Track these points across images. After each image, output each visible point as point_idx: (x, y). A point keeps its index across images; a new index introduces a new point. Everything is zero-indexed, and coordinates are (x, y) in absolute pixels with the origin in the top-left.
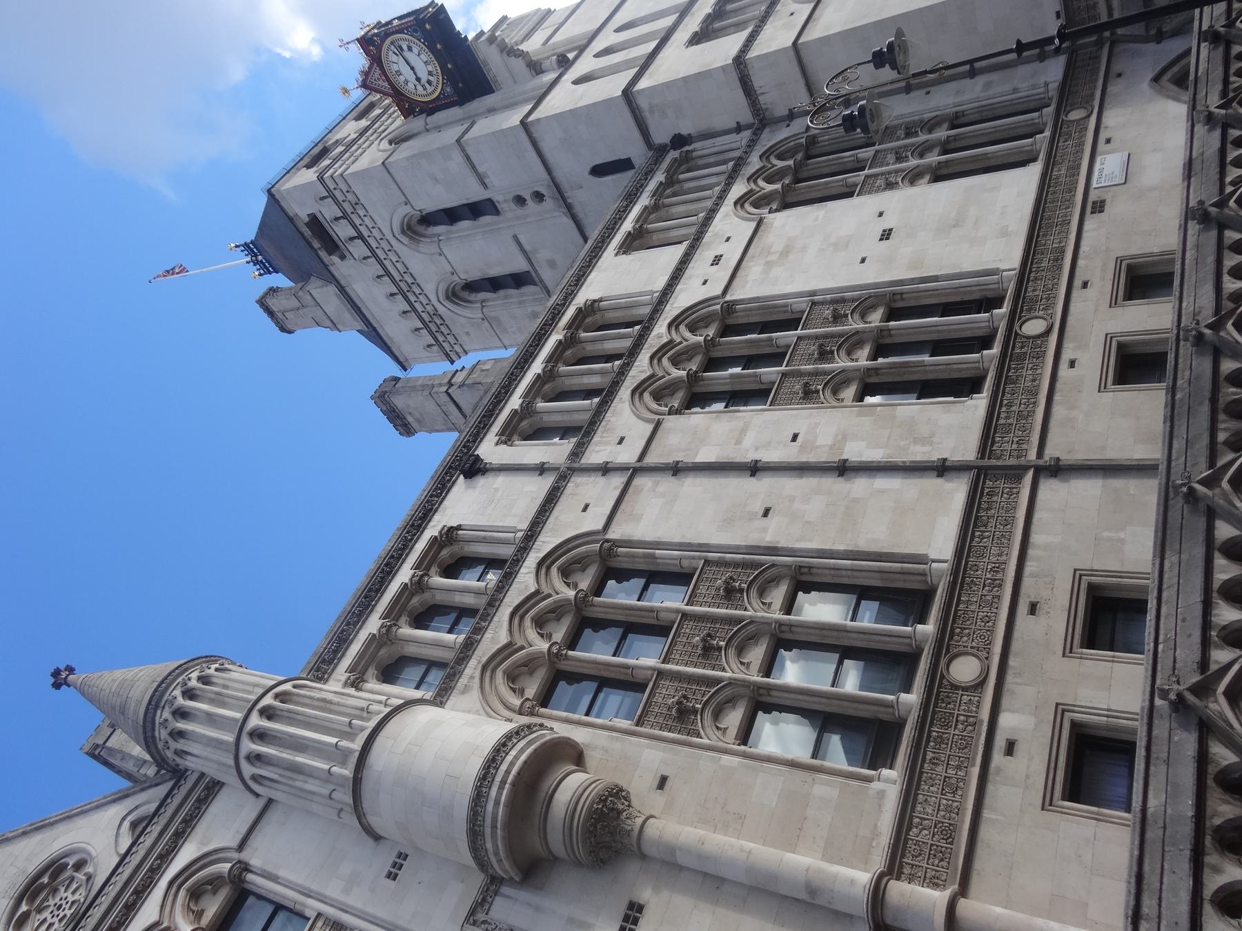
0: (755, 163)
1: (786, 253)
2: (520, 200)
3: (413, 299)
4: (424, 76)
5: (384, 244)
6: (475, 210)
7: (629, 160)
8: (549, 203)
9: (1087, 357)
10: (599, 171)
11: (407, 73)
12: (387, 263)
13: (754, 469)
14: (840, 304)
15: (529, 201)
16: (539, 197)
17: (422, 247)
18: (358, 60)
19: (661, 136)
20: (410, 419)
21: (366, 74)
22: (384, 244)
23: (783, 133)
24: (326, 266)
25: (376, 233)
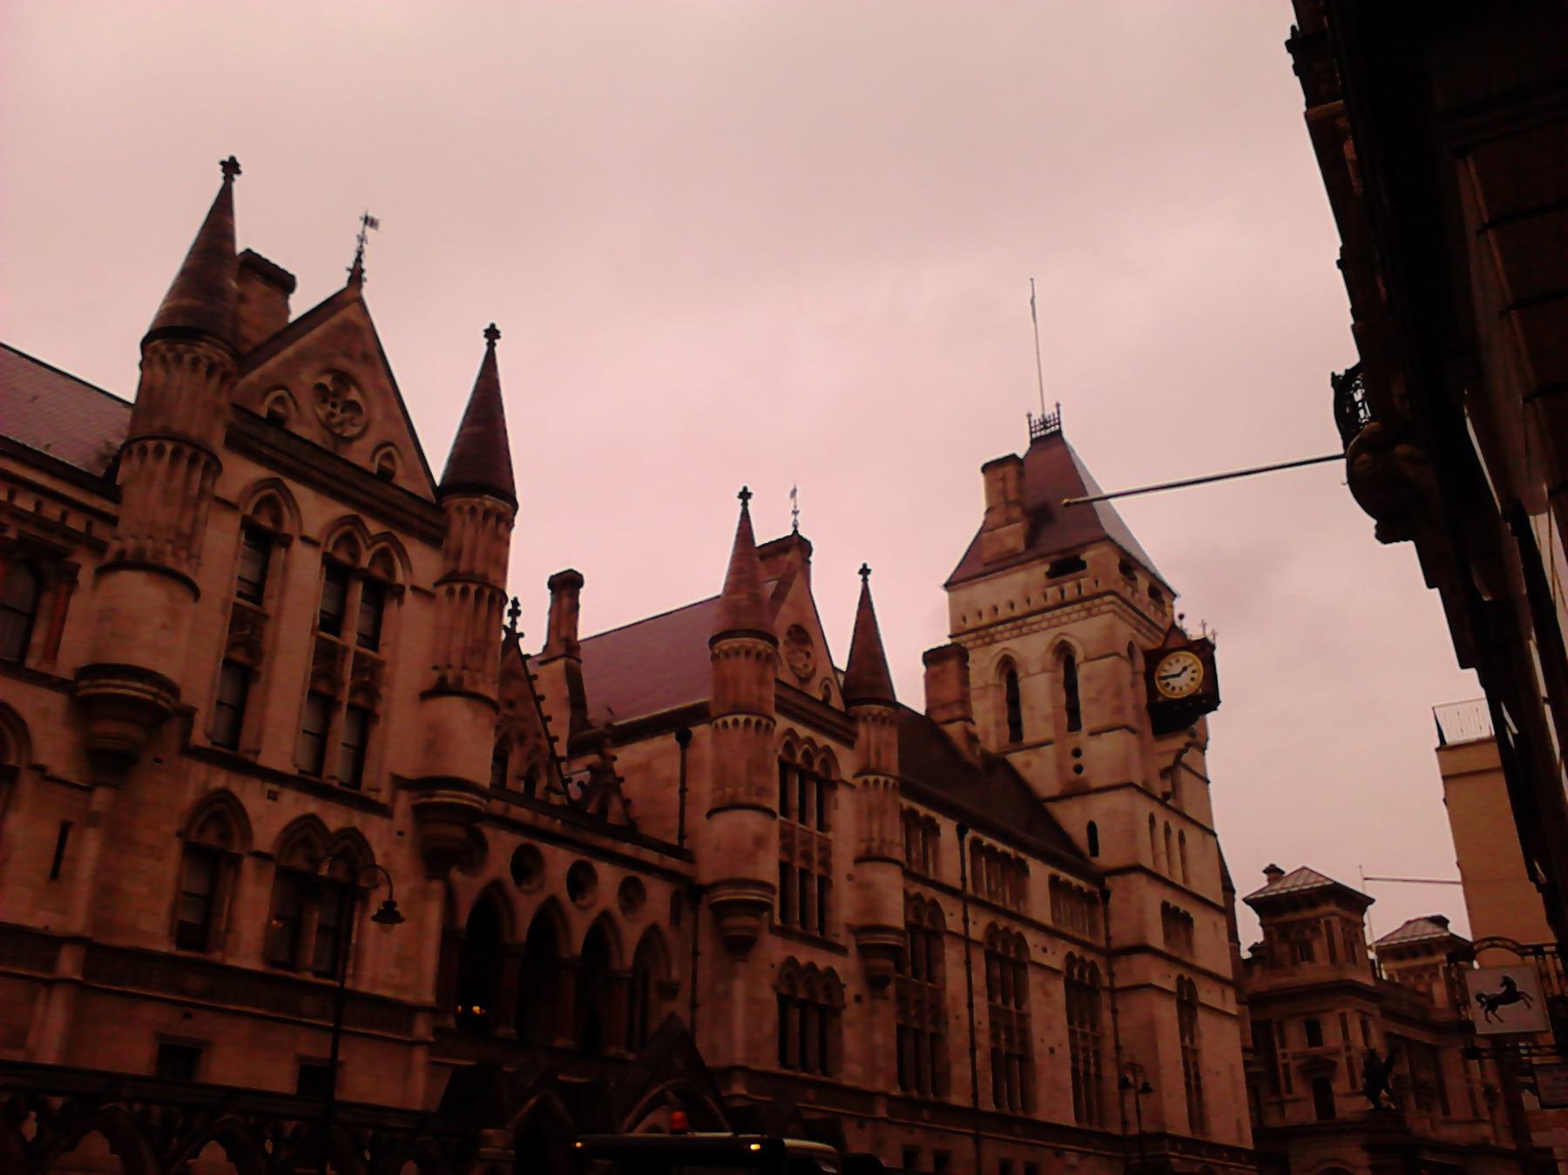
0: (1089, 957)
1: (1047, 994)
2: (1077, 753)
3: (1009, 626)
4: (1172, 681)
5: (1054, 622)
8: (1072, 775)
10: (1092, 828)
11: (1177, 669)
12: (1038, 618)
13: (970, 1006)
14: (1025, 1032)
17: (1050, 656)
18: (1194, 631)
21: (1181, 633)
23: (1102, 971)
25: (1064, 619)
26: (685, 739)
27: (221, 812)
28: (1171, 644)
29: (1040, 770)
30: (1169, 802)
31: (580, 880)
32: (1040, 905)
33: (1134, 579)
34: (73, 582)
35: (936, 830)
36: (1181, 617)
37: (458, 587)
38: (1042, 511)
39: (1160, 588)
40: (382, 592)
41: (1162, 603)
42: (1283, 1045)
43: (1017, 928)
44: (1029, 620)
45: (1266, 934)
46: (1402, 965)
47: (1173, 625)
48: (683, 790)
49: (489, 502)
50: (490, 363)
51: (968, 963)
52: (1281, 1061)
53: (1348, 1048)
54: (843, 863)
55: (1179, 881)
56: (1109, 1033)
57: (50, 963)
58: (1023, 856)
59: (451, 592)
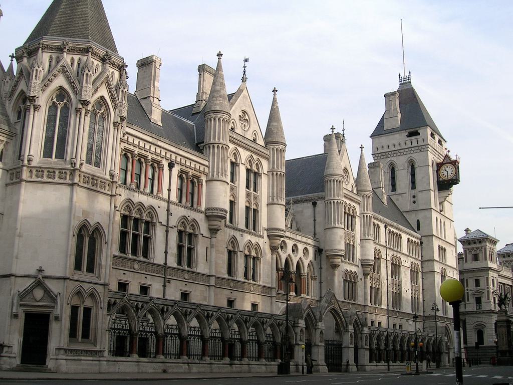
1: (406, 274)
2: (414, 197)
3: (393, 152)
5: (409, 153)
6: (413, 183)
7: (419, 230)
9: (395, 321)
10: (418, 221)
12: (403, 151)
15: (414, 199)
16: (414, 202)
19: (424, 239)
20: (373, 170)
21: (449, 158)
22: (409, 153)
24: (405, 130)
25: (412, 152)
26: (315, 204)
27: (234, 241)
28: (445, 162)
29: (404, 203)
30: (441, 213)
31: (295, 249)
32: (405, 250)
33: (434, 138)
34: (202, 184)
35: (379, 227)
36: (449, 151)
37: (275, 173)
38: (407, 114)
39: (442, 140)
40: (257, 175)
41: (441, 145)
42: (467, 287)
43: (399, 255)
44: (400, 151)
45: (465, 251)
46: (504, 259)
47: (446, 155)
48: (315, 220)
49: (281, 147)
50: (274, 101)
51: (387, 267)
52: (466, 291)
53: (488, 288)
54: (358, 241)
55: (443, 239)
56: (421, 285)
57: (208, 282)
58: (401, 233)
59: (273, 174)
